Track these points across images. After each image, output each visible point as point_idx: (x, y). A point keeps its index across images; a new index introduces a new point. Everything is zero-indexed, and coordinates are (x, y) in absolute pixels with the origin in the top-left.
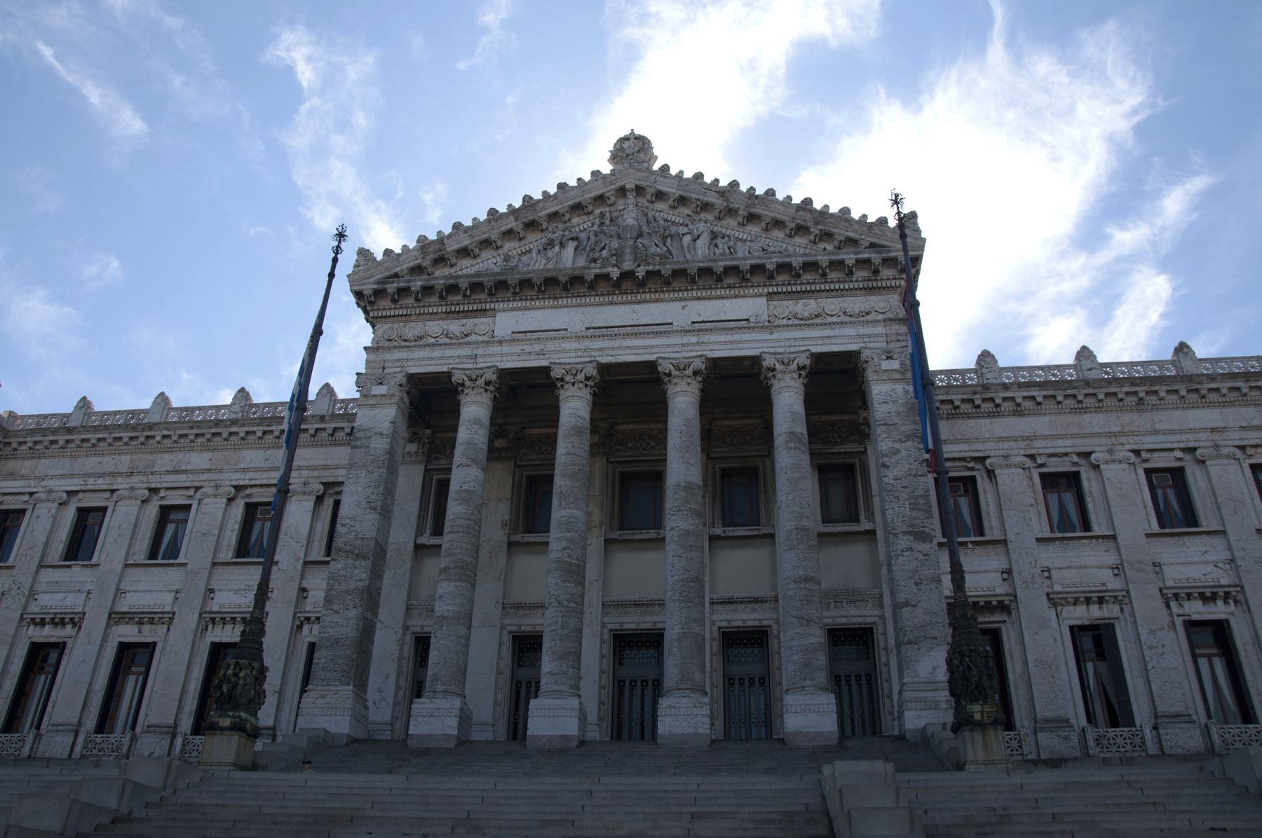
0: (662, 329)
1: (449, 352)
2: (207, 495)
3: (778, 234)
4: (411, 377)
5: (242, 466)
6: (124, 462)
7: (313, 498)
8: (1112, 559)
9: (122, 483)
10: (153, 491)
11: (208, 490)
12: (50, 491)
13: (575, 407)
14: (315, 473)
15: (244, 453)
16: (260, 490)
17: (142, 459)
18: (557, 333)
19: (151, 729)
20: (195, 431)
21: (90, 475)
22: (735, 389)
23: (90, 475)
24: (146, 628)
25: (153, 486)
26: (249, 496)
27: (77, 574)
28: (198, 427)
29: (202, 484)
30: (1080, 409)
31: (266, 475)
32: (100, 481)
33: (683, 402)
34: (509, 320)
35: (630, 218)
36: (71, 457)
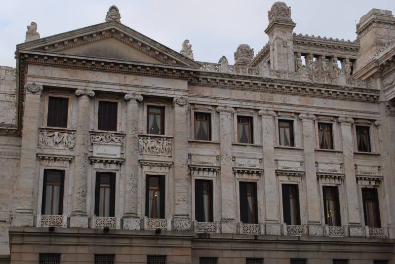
2: (305, 118)
5: (314, 105)
6: (257, 96)
7: (350, 124)
9: (258, 106)
10: (277, 112)
12: (226, 107)
14: (348, 113)
15: (314, 99)
16: (324, 118)
17: (267, 96)
20: (293, 86)
21: (244, 101)
23: (244, 101)
24: (292, 178)
25: (276, 110)
26: (319, 119)
27: (248, 150)
28: (295, 84)
29: (299, 112)
31: (327, 111)
32: (249, 104)
36: (229, 89)
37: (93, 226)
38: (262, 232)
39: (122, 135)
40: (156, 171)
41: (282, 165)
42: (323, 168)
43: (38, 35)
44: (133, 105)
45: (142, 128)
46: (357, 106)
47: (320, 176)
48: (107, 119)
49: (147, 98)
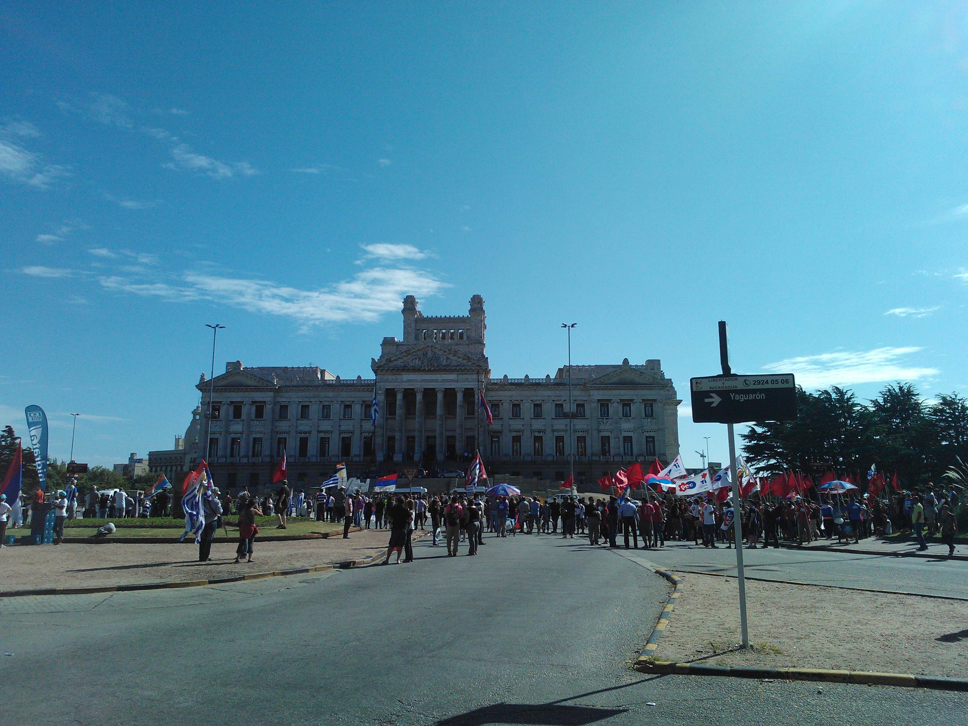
0: (437, 381)
1: (393, 384)
3: (461, 359)
4: (386, 389)
6: (312, 394)
8: (523, 423)
9: (312, 400)
11: (335, 402)
13: (419, 397)
18: (416, 381)
19: (334, 456)
22: (450, 394)
27: (305, 422)
30: (523, 390)
33: (440, 396)
34: (406, 377)
35: (429, 354)
37: (228, 462)
38: (307, 460)
39: (244, 420)
40: (258, 436)
41: (322, 428)
42: (343, 428)
43: (204, 379)
44: (247, 406)
45: (253, 416)
46: (366, 394)
47: (341, 432)
48: (237, 413)
49: (254, 402)
